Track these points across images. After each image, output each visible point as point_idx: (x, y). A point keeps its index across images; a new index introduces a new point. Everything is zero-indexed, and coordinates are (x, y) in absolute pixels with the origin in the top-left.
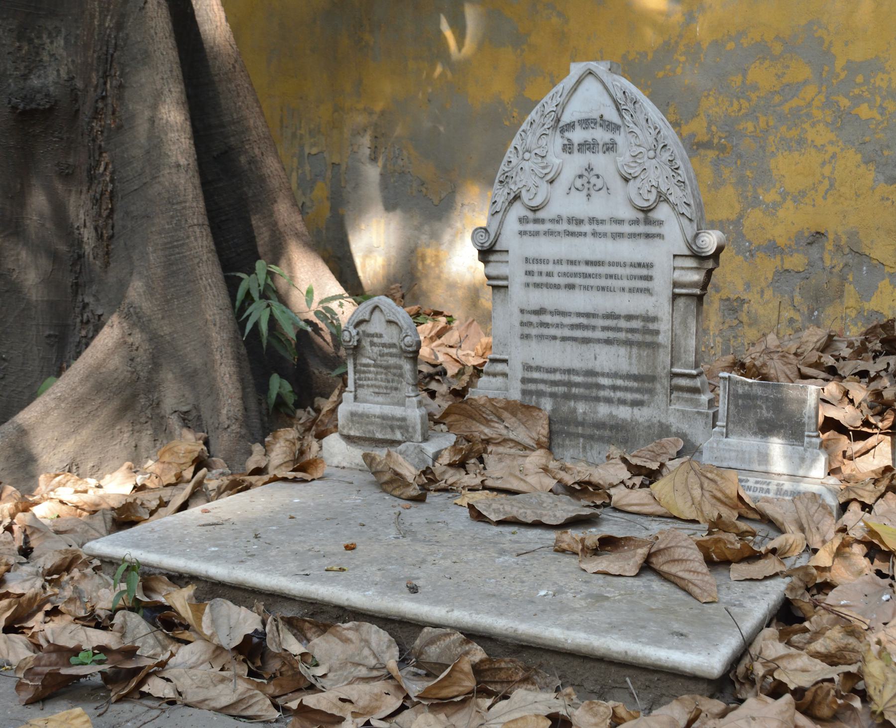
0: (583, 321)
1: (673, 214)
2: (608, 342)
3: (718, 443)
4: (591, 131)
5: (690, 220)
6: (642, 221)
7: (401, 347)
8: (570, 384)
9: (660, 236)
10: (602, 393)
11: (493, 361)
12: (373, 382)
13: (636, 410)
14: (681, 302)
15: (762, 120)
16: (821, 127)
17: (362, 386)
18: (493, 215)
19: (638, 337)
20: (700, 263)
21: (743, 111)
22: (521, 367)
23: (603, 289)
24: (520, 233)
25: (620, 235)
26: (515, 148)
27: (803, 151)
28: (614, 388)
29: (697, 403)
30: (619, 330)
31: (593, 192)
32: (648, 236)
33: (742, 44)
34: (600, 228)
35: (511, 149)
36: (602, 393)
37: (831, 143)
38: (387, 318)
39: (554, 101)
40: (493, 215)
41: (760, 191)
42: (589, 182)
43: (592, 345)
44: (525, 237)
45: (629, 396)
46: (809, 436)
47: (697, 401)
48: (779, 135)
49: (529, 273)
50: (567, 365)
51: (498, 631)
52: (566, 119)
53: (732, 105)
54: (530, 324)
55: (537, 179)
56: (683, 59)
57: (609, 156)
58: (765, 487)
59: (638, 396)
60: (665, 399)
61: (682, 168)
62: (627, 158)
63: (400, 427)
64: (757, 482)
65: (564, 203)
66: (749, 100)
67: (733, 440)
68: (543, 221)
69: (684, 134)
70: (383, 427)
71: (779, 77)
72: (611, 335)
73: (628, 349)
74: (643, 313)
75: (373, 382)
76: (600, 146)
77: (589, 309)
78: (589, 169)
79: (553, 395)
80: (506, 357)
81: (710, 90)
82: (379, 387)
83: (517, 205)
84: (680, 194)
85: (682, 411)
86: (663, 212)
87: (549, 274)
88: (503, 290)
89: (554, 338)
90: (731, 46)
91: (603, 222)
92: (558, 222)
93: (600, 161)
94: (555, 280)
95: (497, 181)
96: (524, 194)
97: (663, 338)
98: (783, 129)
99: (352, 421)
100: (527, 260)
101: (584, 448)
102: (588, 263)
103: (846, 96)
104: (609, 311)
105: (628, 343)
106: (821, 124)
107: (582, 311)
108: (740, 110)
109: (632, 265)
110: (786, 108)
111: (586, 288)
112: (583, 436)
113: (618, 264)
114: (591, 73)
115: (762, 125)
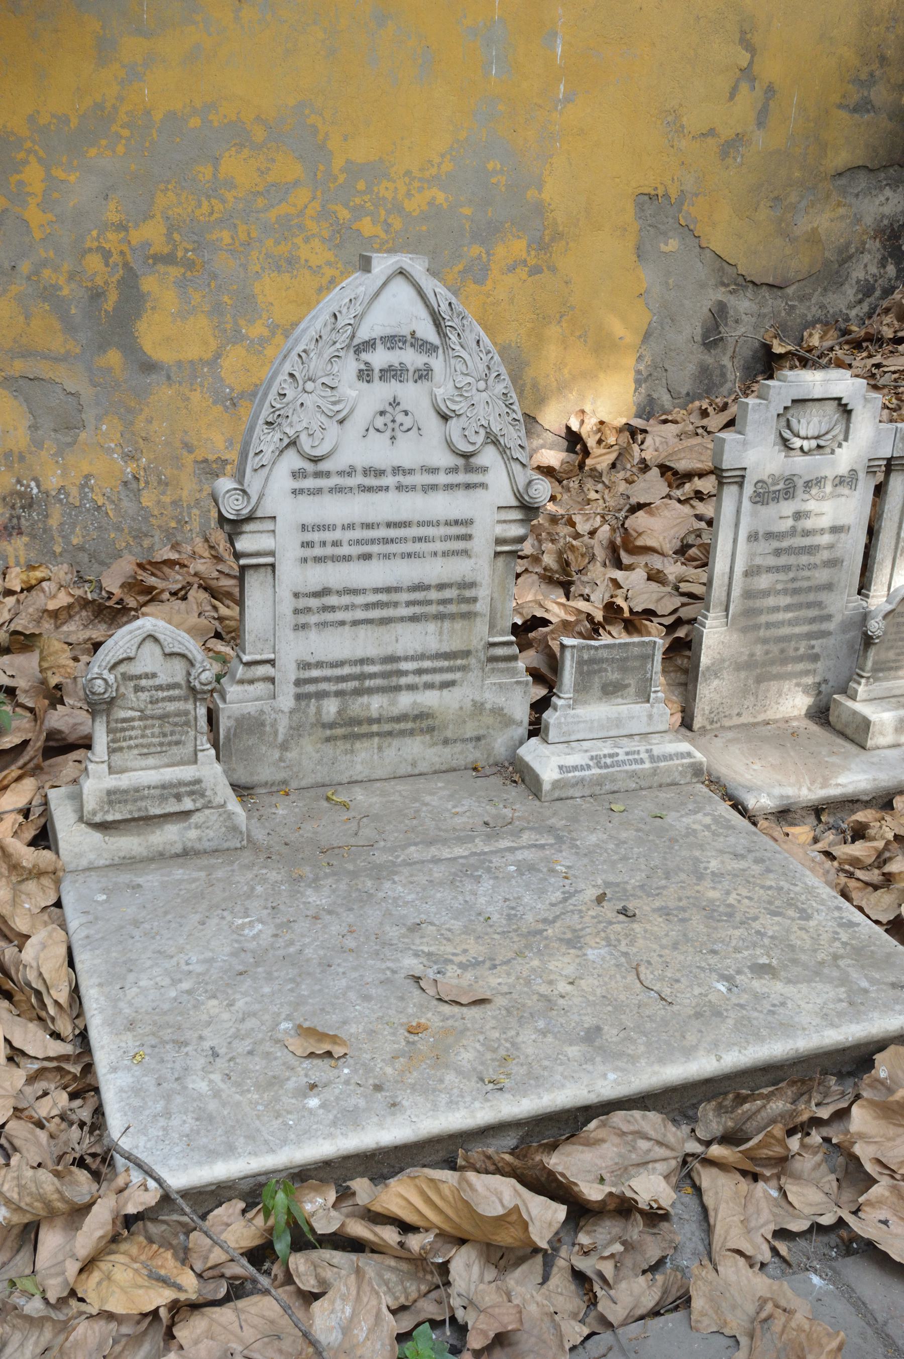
0: (383, 597)
1: (499, 457)
2: (414, 619)
3: (565, 716)
4: (398, 352)
5: (524, 465)
6: (462, 468)
7: (193, 689)
8: (362, 677)
9: (483, 486)
10: (403, 681)
11: (249, 664)
12: (140, 741)
13: (445, 692)
14: (501, 561)
15: (242, 228)
16: (316, 243)
17: (121, 749)
18: (256, 470)
19: (452, 608)
20: (526, 515)
21: (216, 215)
22: (294, 666)
23: (409, 555)
24: (294, 492)
25: (434, 487)
26: (292, 375)
27: (295, 272)
28: (420, 672)
29: (513, 672)
30: (429, 602)
31: (399, 434)
32: (468, 486)
33: (211, 122)
34: (408, 480)
35: (283, 376)
36: (403, 681)
37: (329, 264)
38: (167, 650)
39: (352, 311)
40: (256, 470)
41: (242, 322)
42: (393, 421)
43: (393, 625)
44: (300, 497)
45: (438, 678)
46: (655, 692)
47: (515, 669)
48: (264, 251)
49: (306, 545)
50: (360, 654)
51: (779, 1058)
52: (364, 334)
53: (200, 206)
54: (308, 610)
55: (323, 419)
56: (126, 133)
57: (423, 386)
58: (636, 756)
59: (449, 677)
60: (480, 674)
61: (517, 403)
62: (451, 391)
63: (191, 793)
64: (627, 754)
65: (356, 449)
66: (223, 201)
67: (582, 711)
68: (328, 474)
69: (134, 242)
70: (163, 798)
71: (262, 173)
72: (417, 610)
73: (439, 624)
74: (459, 579)
75: (140, 741)
76: (411, 373)
77: (391, 581)
78: (395, 403)
79: (339, 694)
80: (272, 656)
81: (168, 182)
82: (148, 746)
83: (291, 454)
84: (515, 435)
85: (499, 684)
86: (489, 457)
87: (336, 544)
88: (262, 570)
89: (342, 623)
90: (195, 122)
91: (411, 471)
92: (349, 474)
93: (411, 394)
94: (345, 550)
95: (261, 421)
96: (304, 439)
97: (481, 607)
98: (270, 243)
99: (110, 803)
100: (304, 528)
101: (380, 749)
102: (389, 525)
103: (346, 206)
104: (416, 582)
105: (440, 617)
106: (317, 240)
107: (380, 586)
108: (212, 213)
109: (447, 523)
110: (272, 215)
111: (387, 556)
112: (378, 734)
113: (429, 524)
114: (402, 273)
115: (242, 236)
